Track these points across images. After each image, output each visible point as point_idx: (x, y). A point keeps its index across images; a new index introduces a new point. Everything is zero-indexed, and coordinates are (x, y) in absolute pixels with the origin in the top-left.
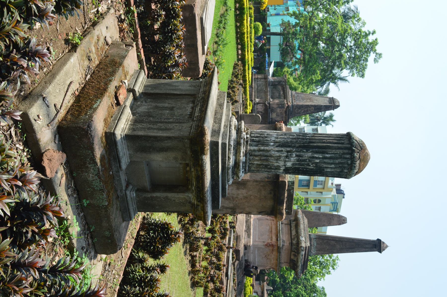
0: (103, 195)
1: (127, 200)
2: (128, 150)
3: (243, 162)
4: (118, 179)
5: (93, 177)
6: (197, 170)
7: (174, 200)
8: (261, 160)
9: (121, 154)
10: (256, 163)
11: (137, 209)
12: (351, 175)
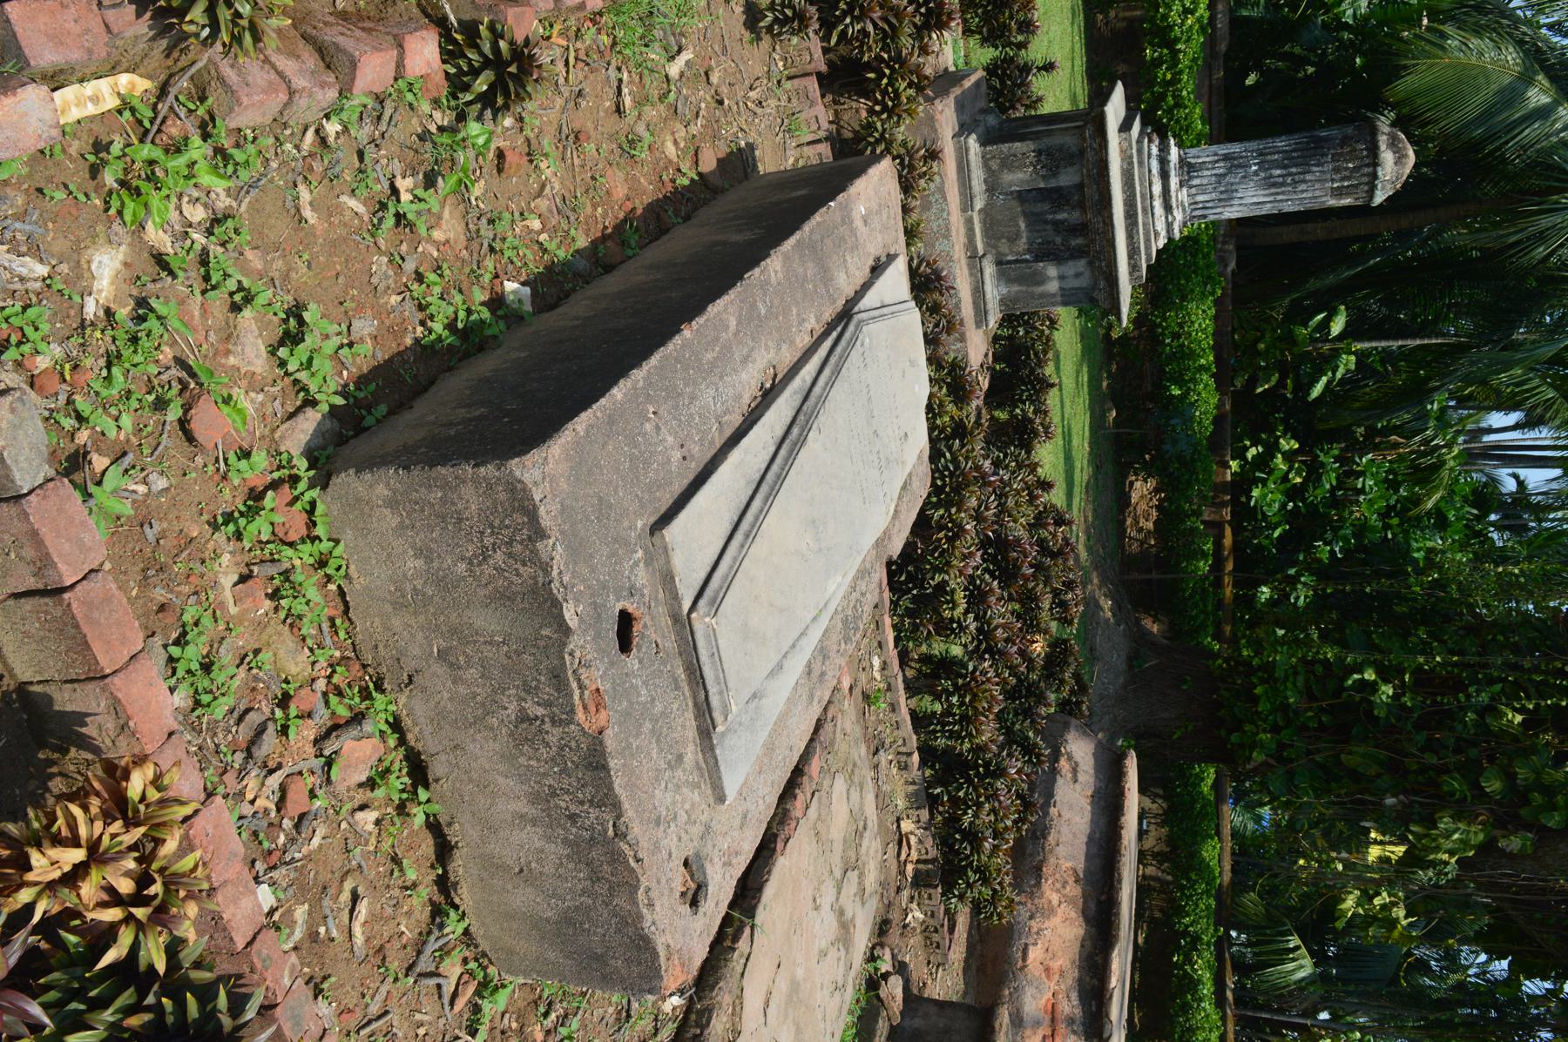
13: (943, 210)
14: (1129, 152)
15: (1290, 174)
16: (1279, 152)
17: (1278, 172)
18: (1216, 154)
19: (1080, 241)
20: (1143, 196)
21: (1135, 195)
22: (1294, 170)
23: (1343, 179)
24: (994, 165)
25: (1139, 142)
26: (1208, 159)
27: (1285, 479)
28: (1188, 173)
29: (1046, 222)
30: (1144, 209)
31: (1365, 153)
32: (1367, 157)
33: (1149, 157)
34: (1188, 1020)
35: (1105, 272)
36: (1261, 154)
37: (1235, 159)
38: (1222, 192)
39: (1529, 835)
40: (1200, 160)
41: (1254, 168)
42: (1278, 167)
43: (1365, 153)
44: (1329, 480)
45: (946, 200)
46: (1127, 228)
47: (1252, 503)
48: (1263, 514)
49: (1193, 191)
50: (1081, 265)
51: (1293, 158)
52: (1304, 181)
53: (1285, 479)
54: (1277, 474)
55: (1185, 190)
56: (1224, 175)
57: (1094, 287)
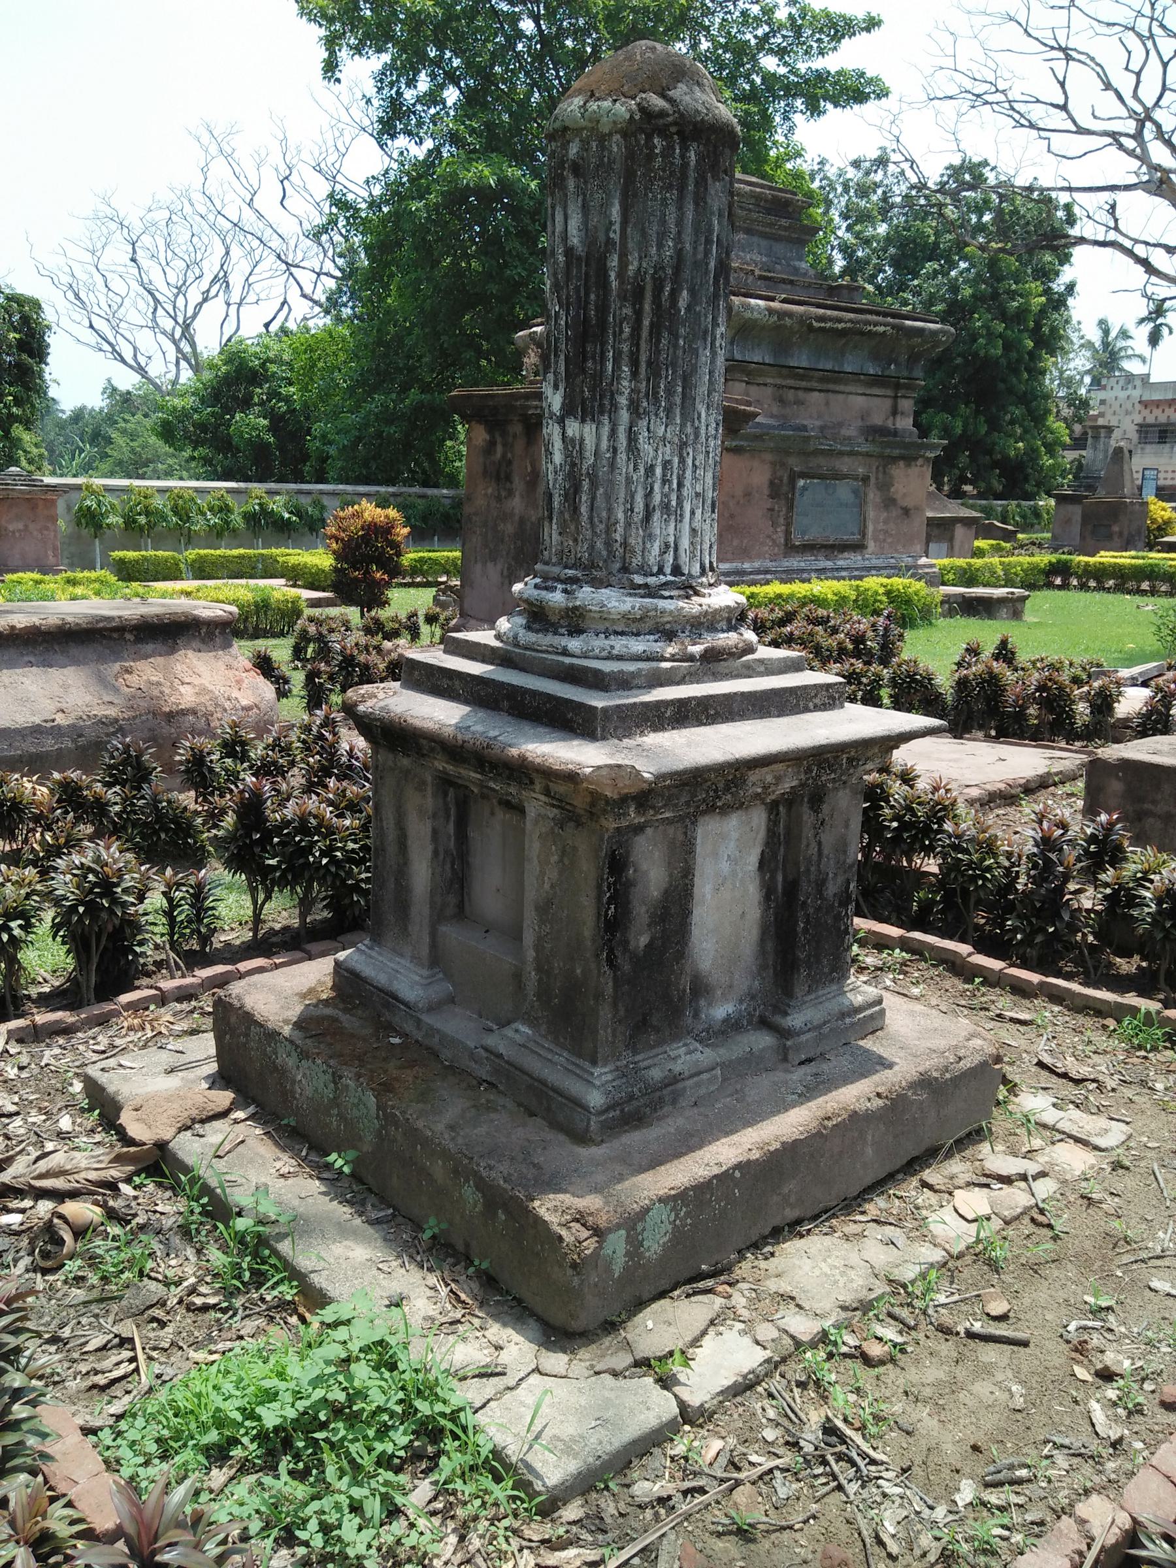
0: (347, 1086)
1: (507, 1062)
2: (402, 955)
3: (536, 586)
4: (436, 1039)
5: (304, 1075)
6: (432, 750)
7: (552, 886)
8: (551, 519)
9: (382, 979)
10: (555, 536)
11: (580, 1062)
12: (590, 121)
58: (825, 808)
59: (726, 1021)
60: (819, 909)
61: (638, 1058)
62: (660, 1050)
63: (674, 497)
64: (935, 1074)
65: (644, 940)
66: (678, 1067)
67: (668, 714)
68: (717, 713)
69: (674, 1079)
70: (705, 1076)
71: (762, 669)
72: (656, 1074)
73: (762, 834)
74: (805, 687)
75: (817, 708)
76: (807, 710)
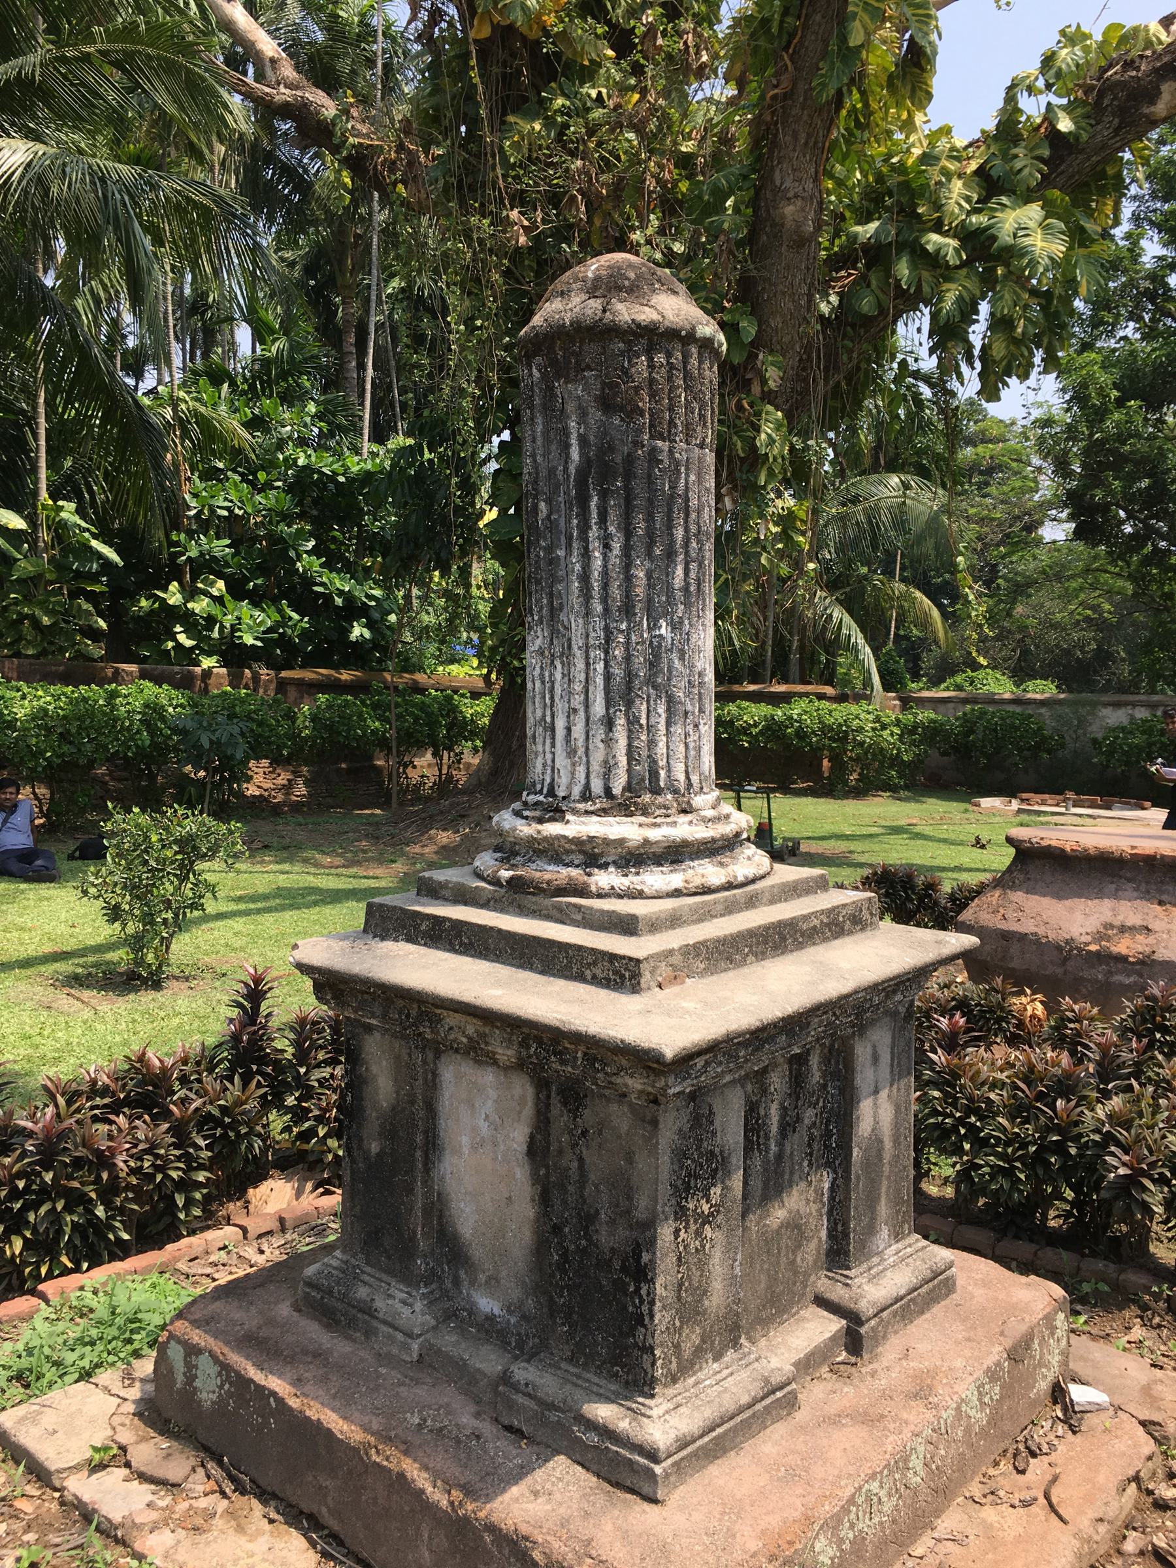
13: (869, 1496)
14: (677, 959)
15: (686, 544)
16: (628, 566)
17: (680, 571)
18: (609, 724)
19: (814, 1061)
20: (730, 909)
21: (751, 933)
22: (679, 533)
23: (702, 416)
24: (691, 1338)
25: (627, 926)
26: (622, 742)
27: (219, 600)
28: (656, 791)
29: (780, 1157)
30: (752, 902)
31: (660, 358)
32: (669, 355)
33: (640, 895)
34: (813, 732)
35: (887, 996)
36: (628, 610)
37: (630, 676)
38: (701, 711)
39: (761, 356)
40: (623, 761)
41: (664, 630)
42: (669, 574)
43: (660, 358)
44: (221, 547)
45: (851, 1501)
46: (800, 946)
47: (259, 644)
48: (269, 630)
49: (695, 779)
50: (862, 1052)
51: (650, 534)
52: (699, 511)
53: (219, 600)
54: (216, 611)
55: (698, 801)
56: (671, 701)
57: (894, 1014)
58: (588, 1116)
59: (490, 1318)
60: (583, 1252)
61: (368, 1269)
62: (384, 1277)
63: (548, 713)
64: (537, 1555)
65: (375, 1147)
66: (380, 1304)
67: (423, 927)
68: (471, 943)
69: (368, 1310)
70: (400, 1336)
71: (579, 917)
72: (362, 1292)
73: (529, 1110)
74: (580, 948)
75: (595, 981)
76: (580, 978)
